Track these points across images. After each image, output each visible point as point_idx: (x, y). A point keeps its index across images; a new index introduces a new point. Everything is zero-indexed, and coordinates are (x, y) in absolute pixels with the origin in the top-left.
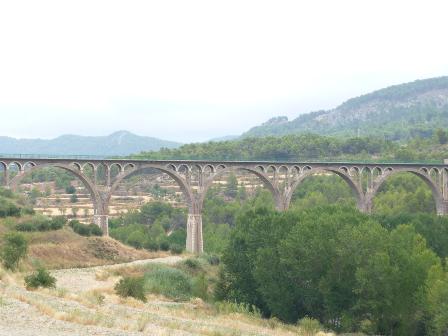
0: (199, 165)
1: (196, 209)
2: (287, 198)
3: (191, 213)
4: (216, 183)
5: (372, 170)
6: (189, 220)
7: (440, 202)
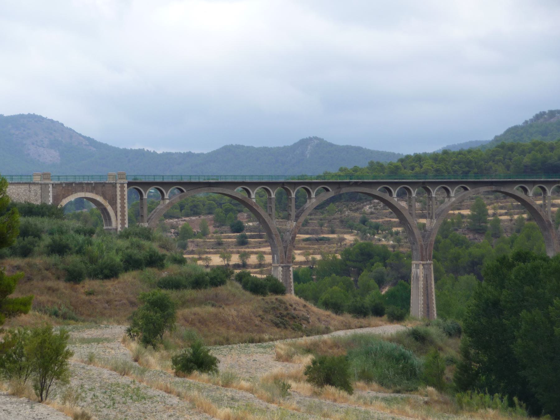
1: (424, 253)
3: (417, 260)
6: (414, 270)
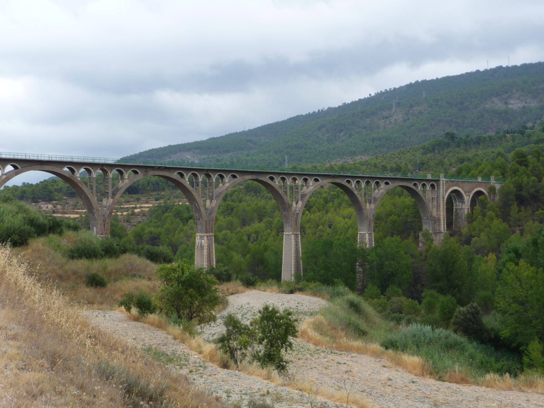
0: (210, 174)
1: (208, 227)
2: (297, 214)
3: (201, 232)
4: (82, 212)
5: (373, 184)
6: (198, 241)
7: (428, 219)
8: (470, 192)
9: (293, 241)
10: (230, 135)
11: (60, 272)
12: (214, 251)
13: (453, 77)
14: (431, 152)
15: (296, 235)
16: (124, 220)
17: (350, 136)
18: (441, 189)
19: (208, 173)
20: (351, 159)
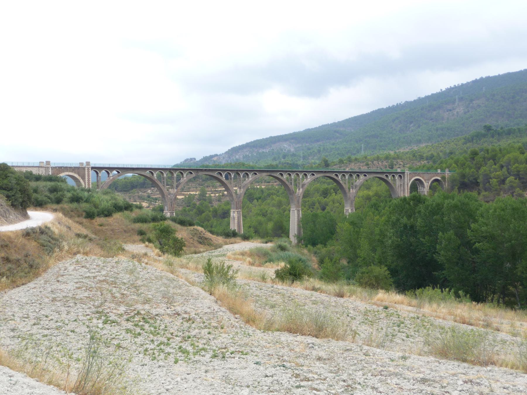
5: (354, 176)
6: (232, 214)
8: (429, 180)
9: (296, 214)
10: (323, 126)
11: (125, 229)
12: (242, 220)
13: (513, 73)
14: (470, 142)
15: (298, 211)
16: (216, 200)
17: (419, 127)
18: (406, 179)
19: (237, 172)
20: (416, 146)
